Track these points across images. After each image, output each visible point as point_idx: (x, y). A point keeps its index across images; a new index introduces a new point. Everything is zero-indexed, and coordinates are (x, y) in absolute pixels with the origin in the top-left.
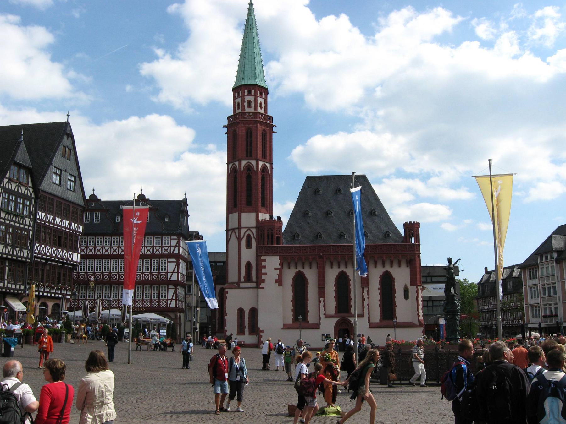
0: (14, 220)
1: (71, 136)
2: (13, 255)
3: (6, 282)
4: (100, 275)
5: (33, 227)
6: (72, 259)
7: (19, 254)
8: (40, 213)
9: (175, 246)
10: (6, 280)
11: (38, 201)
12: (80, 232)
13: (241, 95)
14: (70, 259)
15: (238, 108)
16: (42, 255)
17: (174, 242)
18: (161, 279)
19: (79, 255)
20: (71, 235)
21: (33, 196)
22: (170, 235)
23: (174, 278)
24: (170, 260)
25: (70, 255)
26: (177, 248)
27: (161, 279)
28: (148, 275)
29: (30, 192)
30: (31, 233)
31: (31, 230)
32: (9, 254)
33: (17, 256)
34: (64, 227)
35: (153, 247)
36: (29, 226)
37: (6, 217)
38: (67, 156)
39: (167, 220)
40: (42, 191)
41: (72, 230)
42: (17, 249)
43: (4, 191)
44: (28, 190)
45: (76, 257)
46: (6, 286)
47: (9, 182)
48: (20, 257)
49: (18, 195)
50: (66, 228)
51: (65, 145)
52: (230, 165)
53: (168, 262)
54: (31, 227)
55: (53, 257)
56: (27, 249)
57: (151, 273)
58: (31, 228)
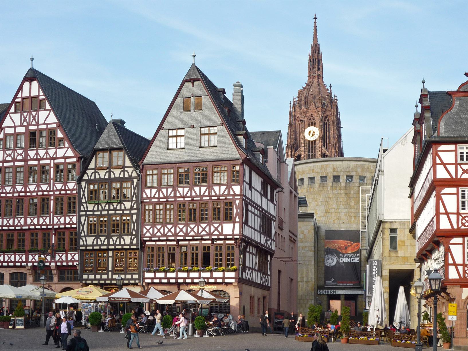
0: (107, 208)
2: (109, 244)
3: (110, 273)
5: (137, 209)
6: (221, 234)
7: (118, 243)
8: (148, 191)
10: (110, 271)
12: (235, 195)
14: (216, 233)
16: (159, 237)
19: (237, 226)
25: (216, 229)
30: (134, 217)
31: (134, 214)
32: (103, 245)
33: (115, 244)
34: (197, 196)
36: (132, 209)
37: (96, 208)
38: (192, 107)
41: (216, 195)
42: (115, 238)
46: (110, 277)
47: (95, 173)
48: (120, 244)
49: (111, 181)
50: (200, 196)
54: (135, 209)
55: (181, 236)
56: (131, 235)
58: (133, 212)
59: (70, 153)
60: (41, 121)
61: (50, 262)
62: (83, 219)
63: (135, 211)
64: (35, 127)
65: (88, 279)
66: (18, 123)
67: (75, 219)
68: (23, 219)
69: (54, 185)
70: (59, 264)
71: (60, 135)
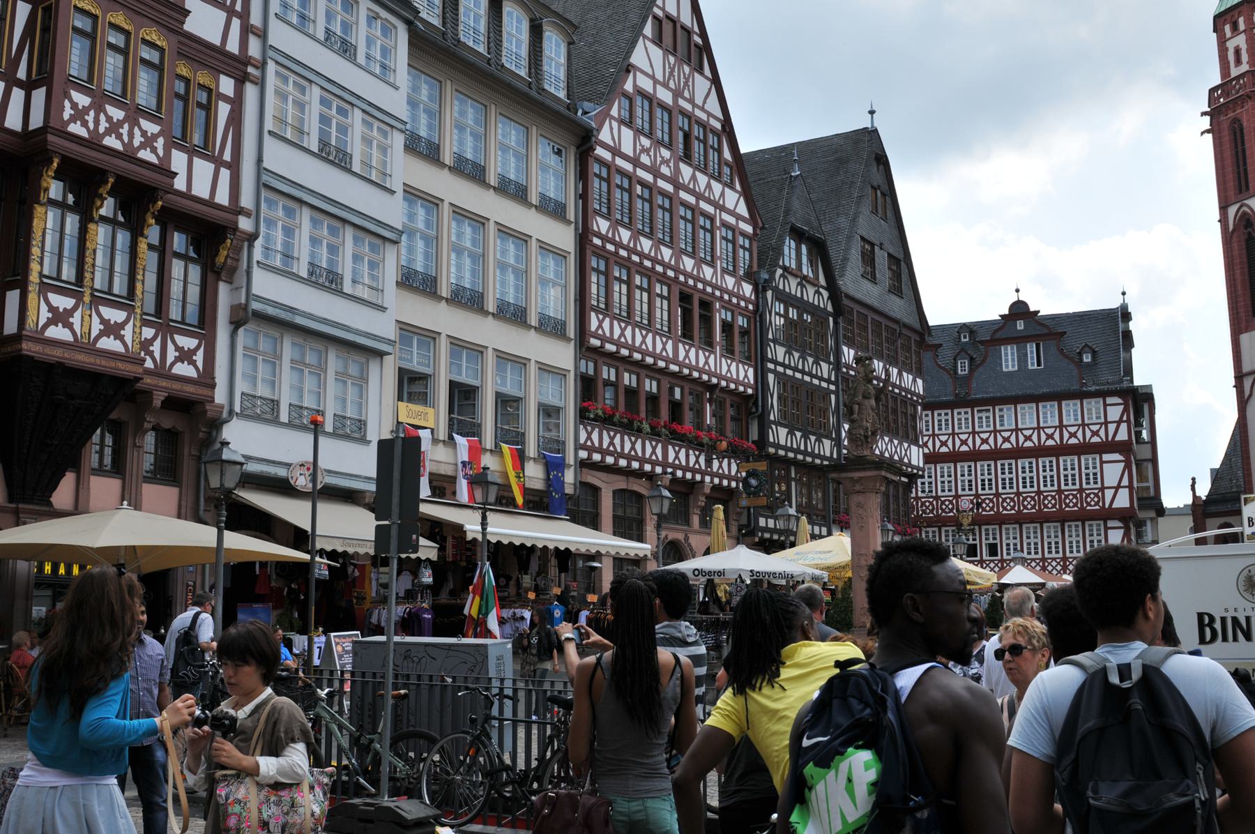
1: (882, 160)
4: (931, 503)
9: (1119, 423)
11: (840, 320)
12: (918, 395)
13: (1242, 27)
15: (1238, 61)
17: (1115, 413)
18: (1089, 504)
20: (904, 401)
21: (830, 308)
22: (1103, 394)
23: (1123, 501)
24: (1106, 457)
26: (1124, 426)
27: (1089, 504)
28: (1054, 497)
29: (823, 300)
30: (833, 397)
31: (832, 392)
35: (1061, 426)
39: (1087, 358)
40: (847, 296)
43: (777, 299)
44: (820, 294)
45: (915, 456)
51: (875, 184)
52: (1232, 211)
53: (1102, 462)
54: (833, 383)
56: (828, 437)
57: (1060, 491)
58: (832, 387)
59: (743, 210)
60: (699, 101)
61: (703, 473)
62: (771, 377)
63: (832, 387)
64: (688, 107)
65: (766, 529)
66: (659, 77)
67: (751, 372)
68: (670, 342)
69: (722, 277)
70: (716, 481)
71: (727, 155)
